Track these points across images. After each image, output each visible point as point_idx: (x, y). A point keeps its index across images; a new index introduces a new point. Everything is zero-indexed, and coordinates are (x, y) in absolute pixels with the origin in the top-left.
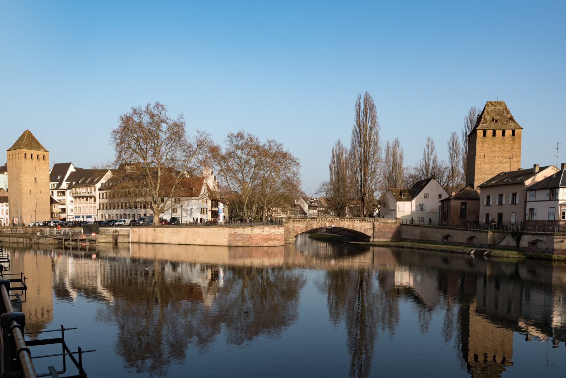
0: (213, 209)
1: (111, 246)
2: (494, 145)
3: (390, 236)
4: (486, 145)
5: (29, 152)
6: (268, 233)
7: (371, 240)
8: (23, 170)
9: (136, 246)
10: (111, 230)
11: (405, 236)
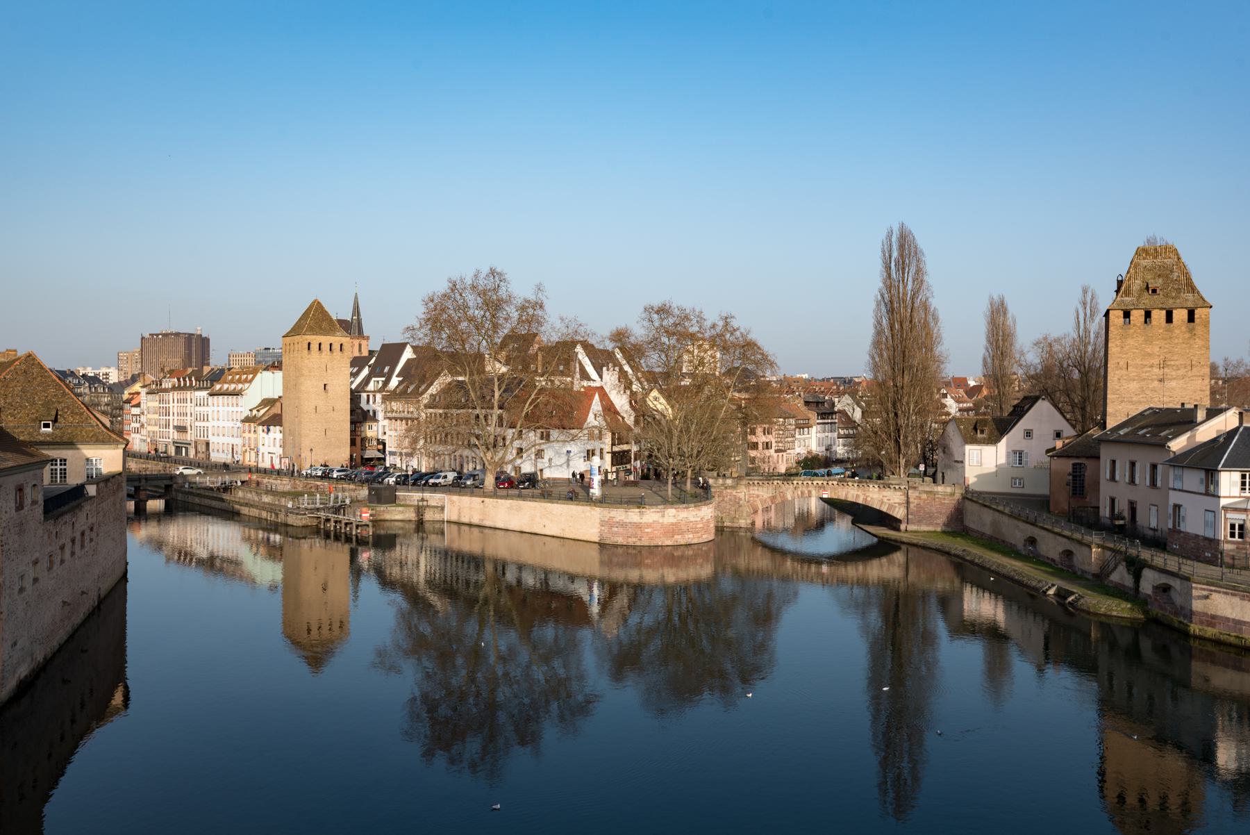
0: (616, 449)
1: (413, 526)
2: (1149, 341)
3: (942, 520)
4: (1131, 342)
5: (315, 339)
6: (674, 521)
7: (903, 527)
8: (305, 372)
9: (454, 527)
10: (415, 496)
11: (971, 522)
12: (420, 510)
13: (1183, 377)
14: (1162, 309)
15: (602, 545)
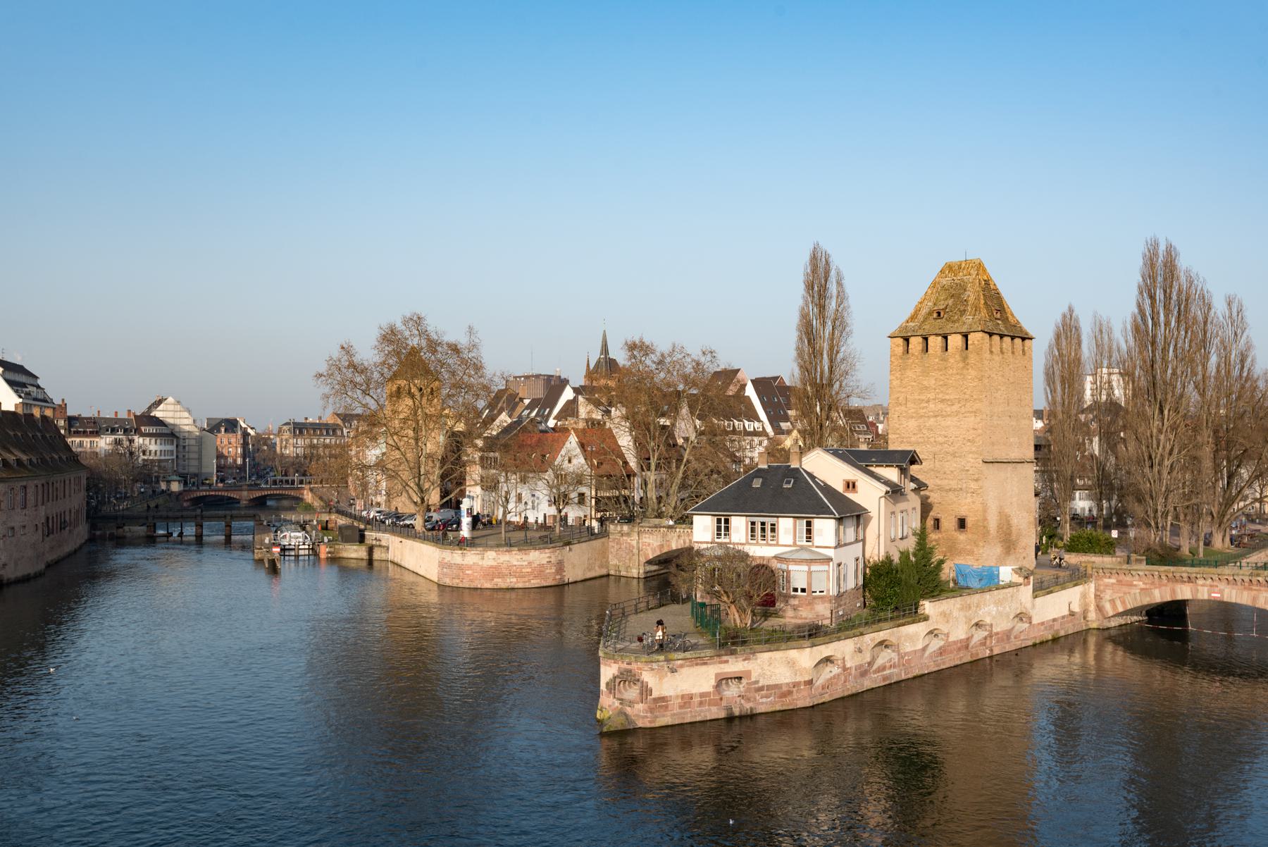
1: (364, 564)
2: (925, 373)
4: (909, 373)
6: (494, 563)
12: (371, 550)
13: (958, 413)
14: (937, 335)
15: (441, 587)
